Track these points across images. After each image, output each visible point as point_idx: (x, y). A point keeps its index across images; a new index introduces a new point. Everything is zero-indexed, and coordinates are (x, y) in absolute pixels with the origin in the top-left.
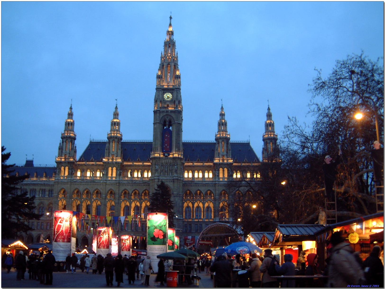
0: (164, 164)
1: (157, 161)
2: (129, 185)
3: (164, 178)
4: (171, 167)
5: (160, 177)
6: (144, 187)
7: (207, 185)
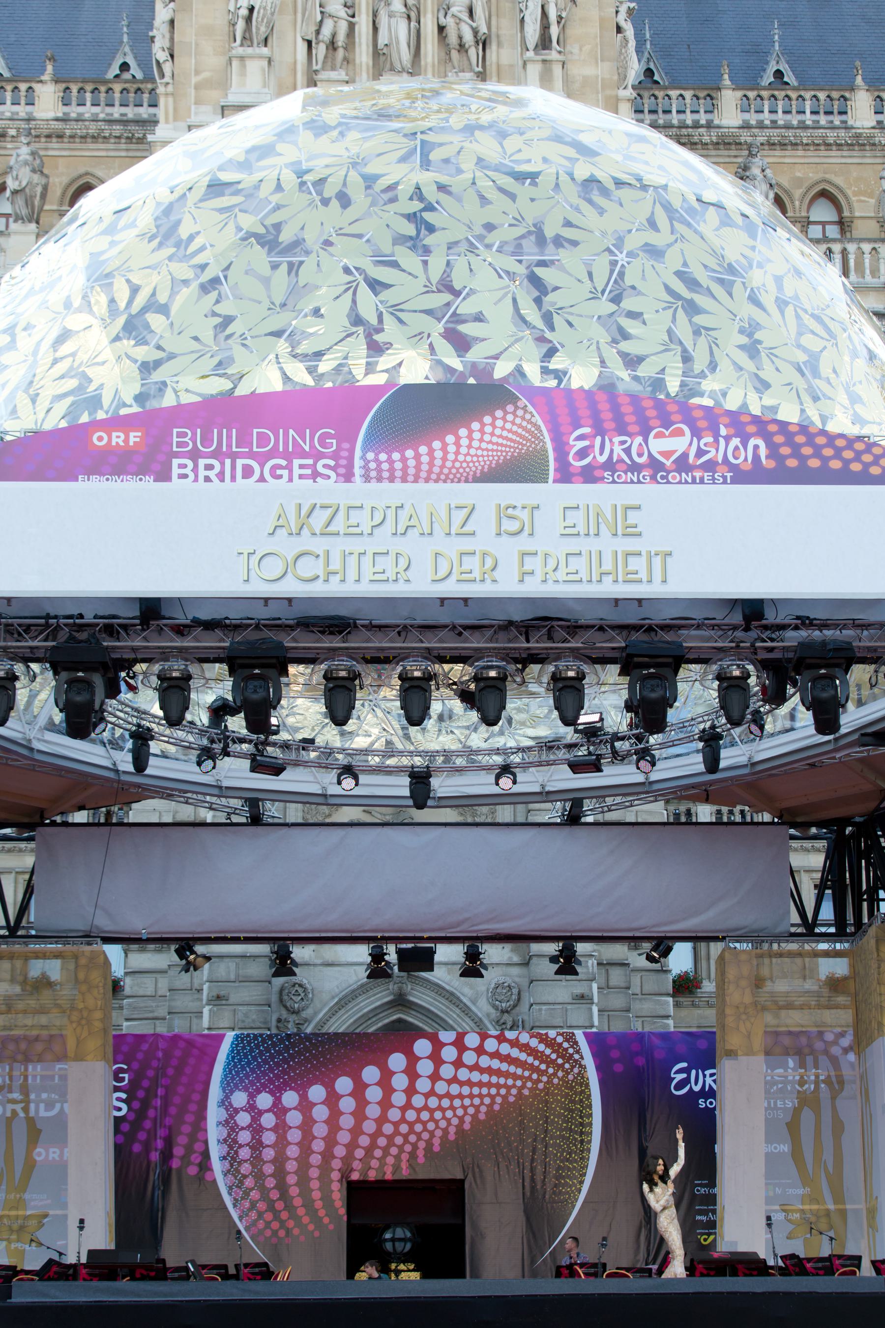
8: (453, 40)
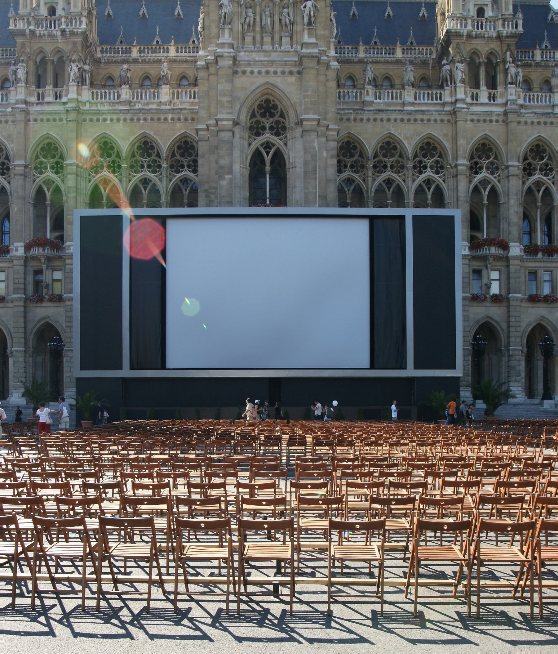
2: (118, 120)
4: (286, 10)
5: (242, 54)
6: (178, 125)
7: (419, 117)
8: (283, 23)
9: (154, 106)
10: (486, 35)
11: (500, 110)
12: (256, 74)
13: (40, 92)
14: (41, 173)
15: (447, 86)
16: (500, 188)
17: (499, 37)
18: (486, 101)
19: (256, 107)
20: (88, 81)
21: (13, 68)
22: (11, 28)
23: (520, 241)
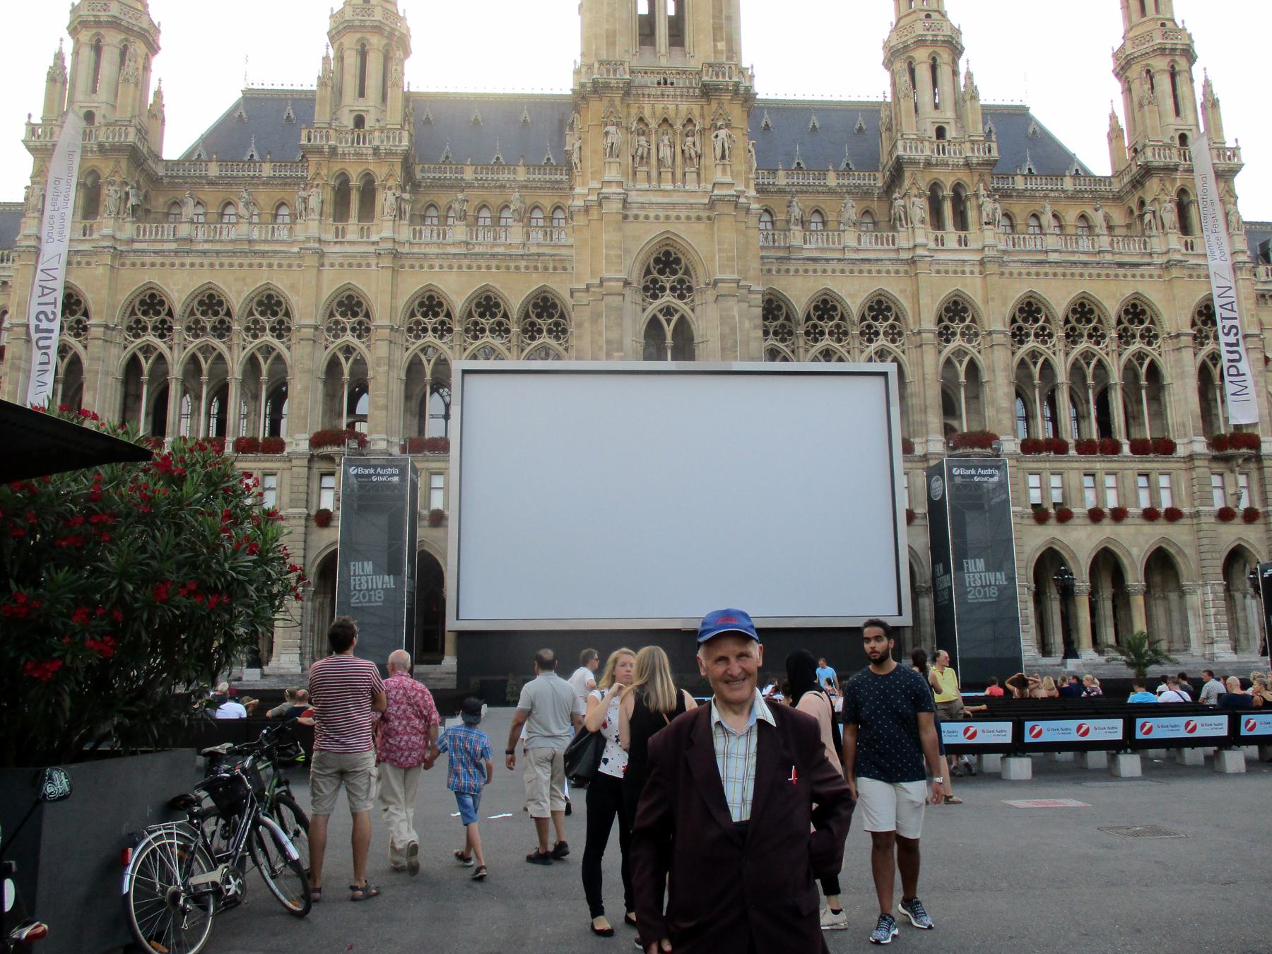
0: (653, 124)
1: (612, 102)
2: (451, 267)
3: (654, 200)
4: (690, 139)
6: (534, 275)
7: (866, 267)
8: (687, 155)
9: (501, 250)
10: (950, 162)
11: (978, 257)
12: (652, 219)
13: (340, 227)
14: (336, 336)
15: (902, 226)
16: (982, 361)
17: (967, 165)
18: (956, 246)
19: (652, 261)
20: (408, 215)
21: (303, 194)
22: (302, 142)
23: (1015, 434)
